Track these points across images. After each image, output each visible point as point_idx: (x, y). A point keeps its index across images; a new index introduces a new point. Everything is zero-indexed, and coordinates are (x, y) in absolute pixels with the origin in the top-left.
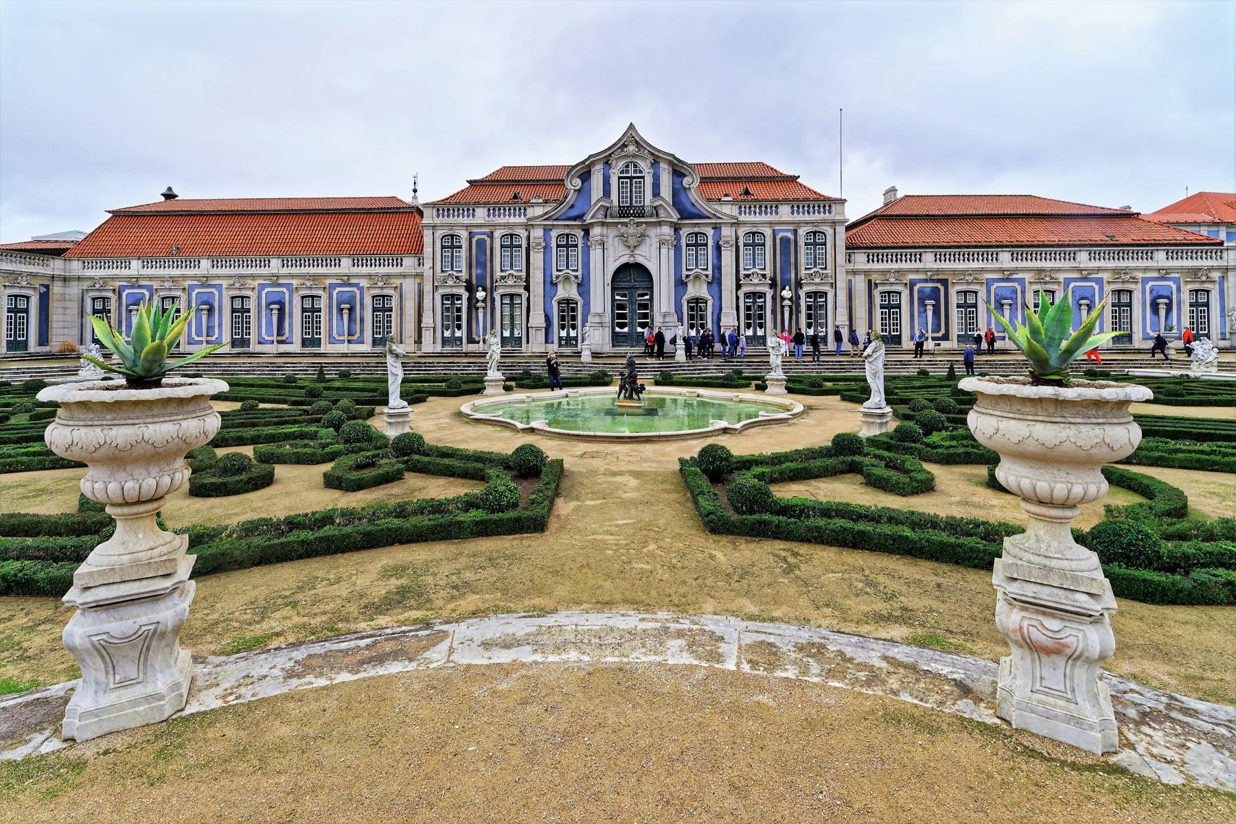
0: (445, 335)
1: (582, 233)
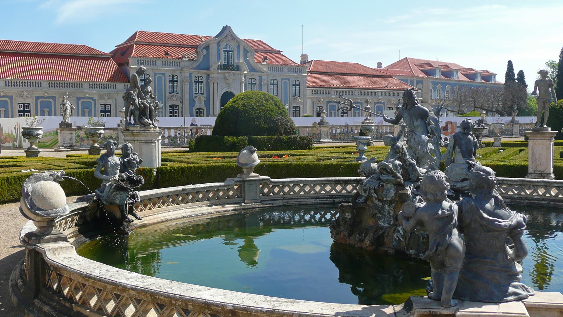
1: (206, 76)
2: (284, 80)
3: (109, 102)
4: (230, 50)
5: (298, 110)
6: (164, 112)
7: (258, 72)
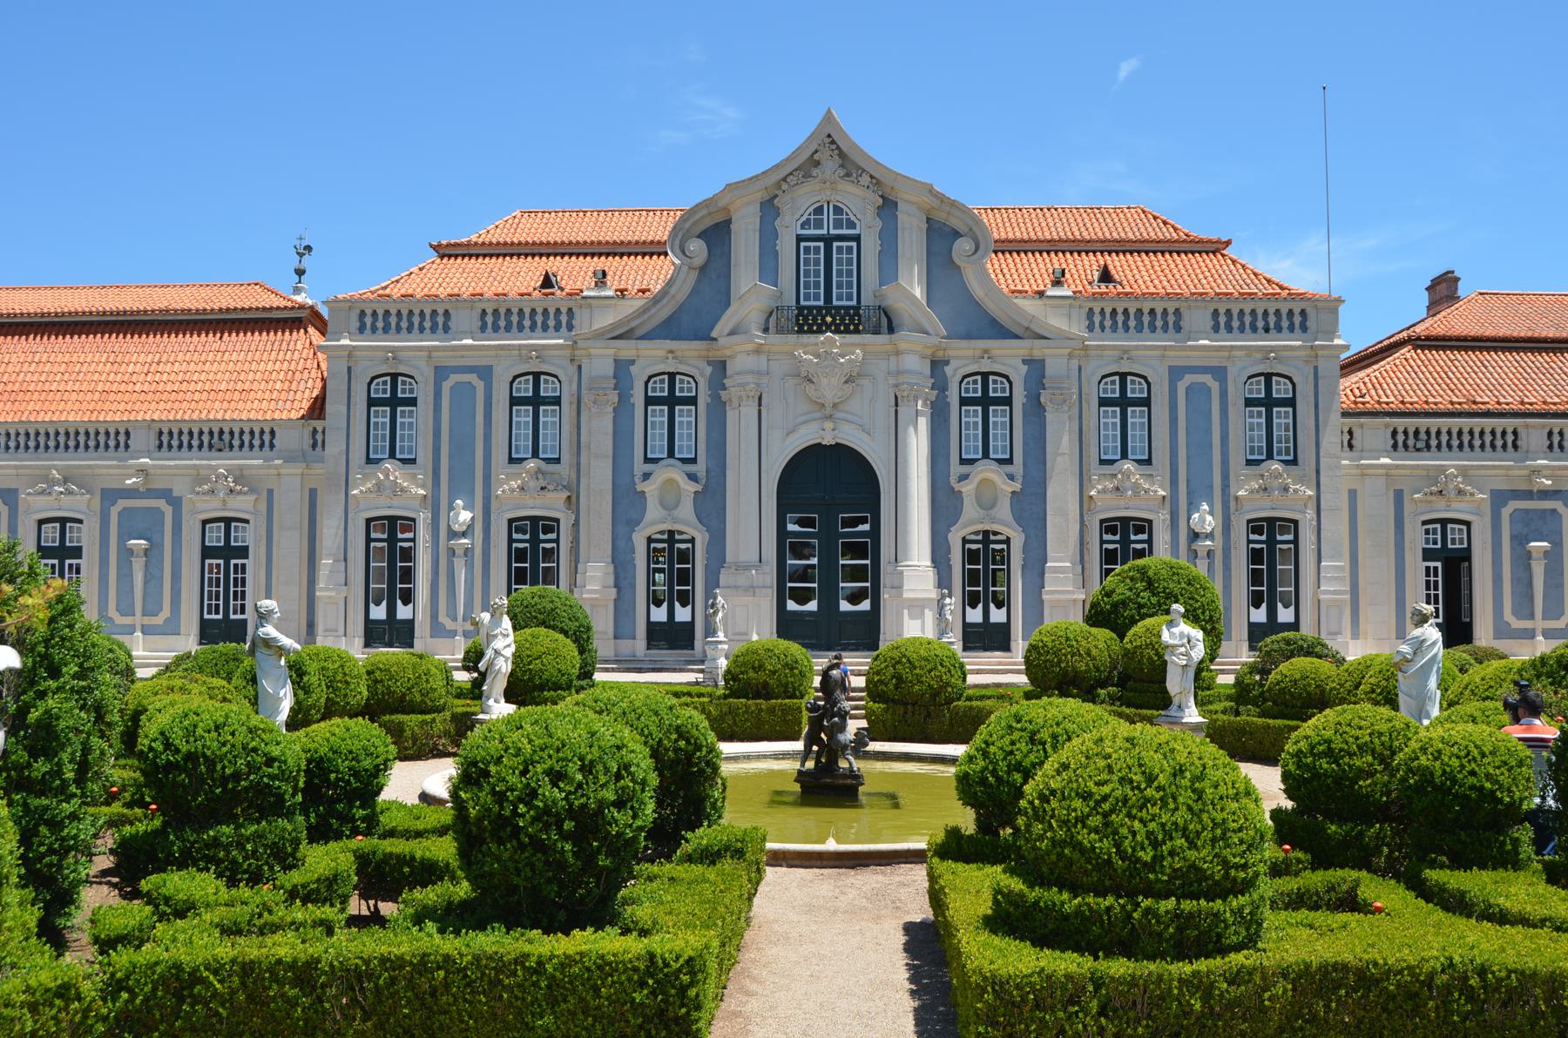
0: (373, 616)
1: (709, 370)
2: (1189, 379)
3: (240, 505)
4: (845, 232)
5: (1290, 537)
6: (478, 551)
7: (1017, 337)
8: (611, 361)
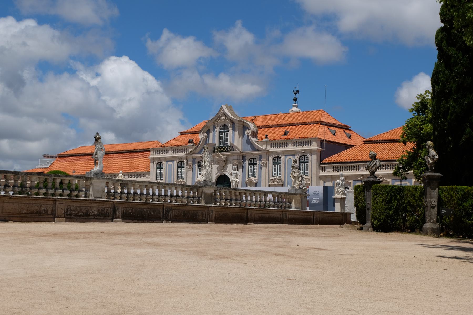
8: (192, 159)
